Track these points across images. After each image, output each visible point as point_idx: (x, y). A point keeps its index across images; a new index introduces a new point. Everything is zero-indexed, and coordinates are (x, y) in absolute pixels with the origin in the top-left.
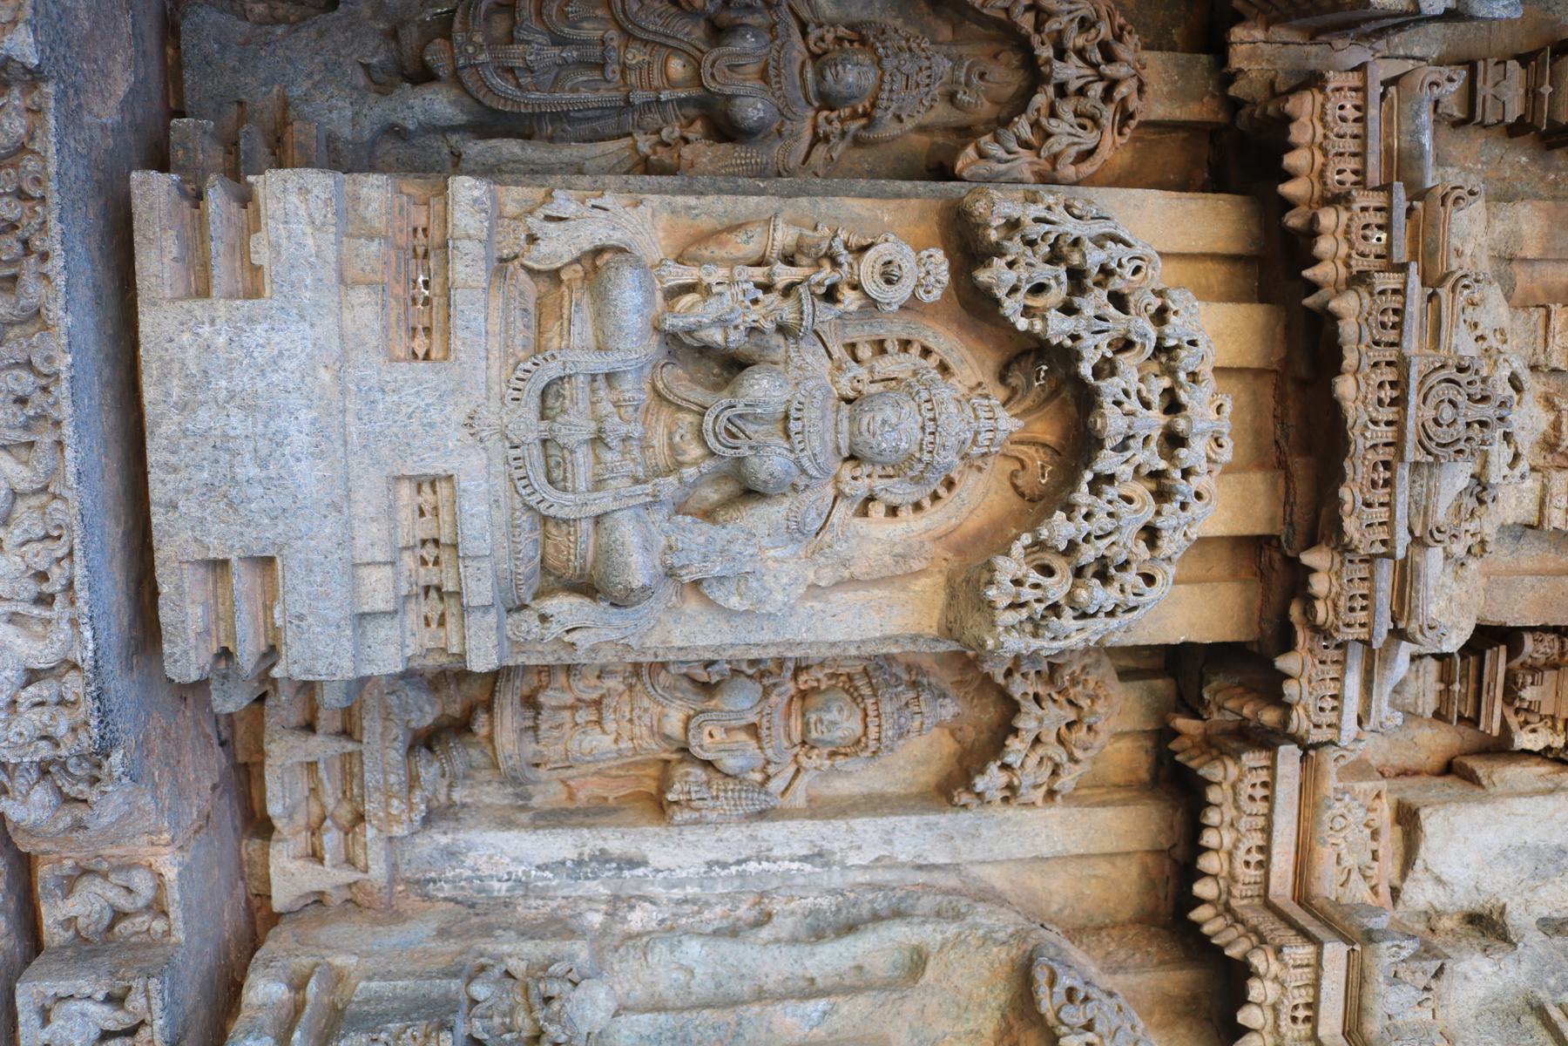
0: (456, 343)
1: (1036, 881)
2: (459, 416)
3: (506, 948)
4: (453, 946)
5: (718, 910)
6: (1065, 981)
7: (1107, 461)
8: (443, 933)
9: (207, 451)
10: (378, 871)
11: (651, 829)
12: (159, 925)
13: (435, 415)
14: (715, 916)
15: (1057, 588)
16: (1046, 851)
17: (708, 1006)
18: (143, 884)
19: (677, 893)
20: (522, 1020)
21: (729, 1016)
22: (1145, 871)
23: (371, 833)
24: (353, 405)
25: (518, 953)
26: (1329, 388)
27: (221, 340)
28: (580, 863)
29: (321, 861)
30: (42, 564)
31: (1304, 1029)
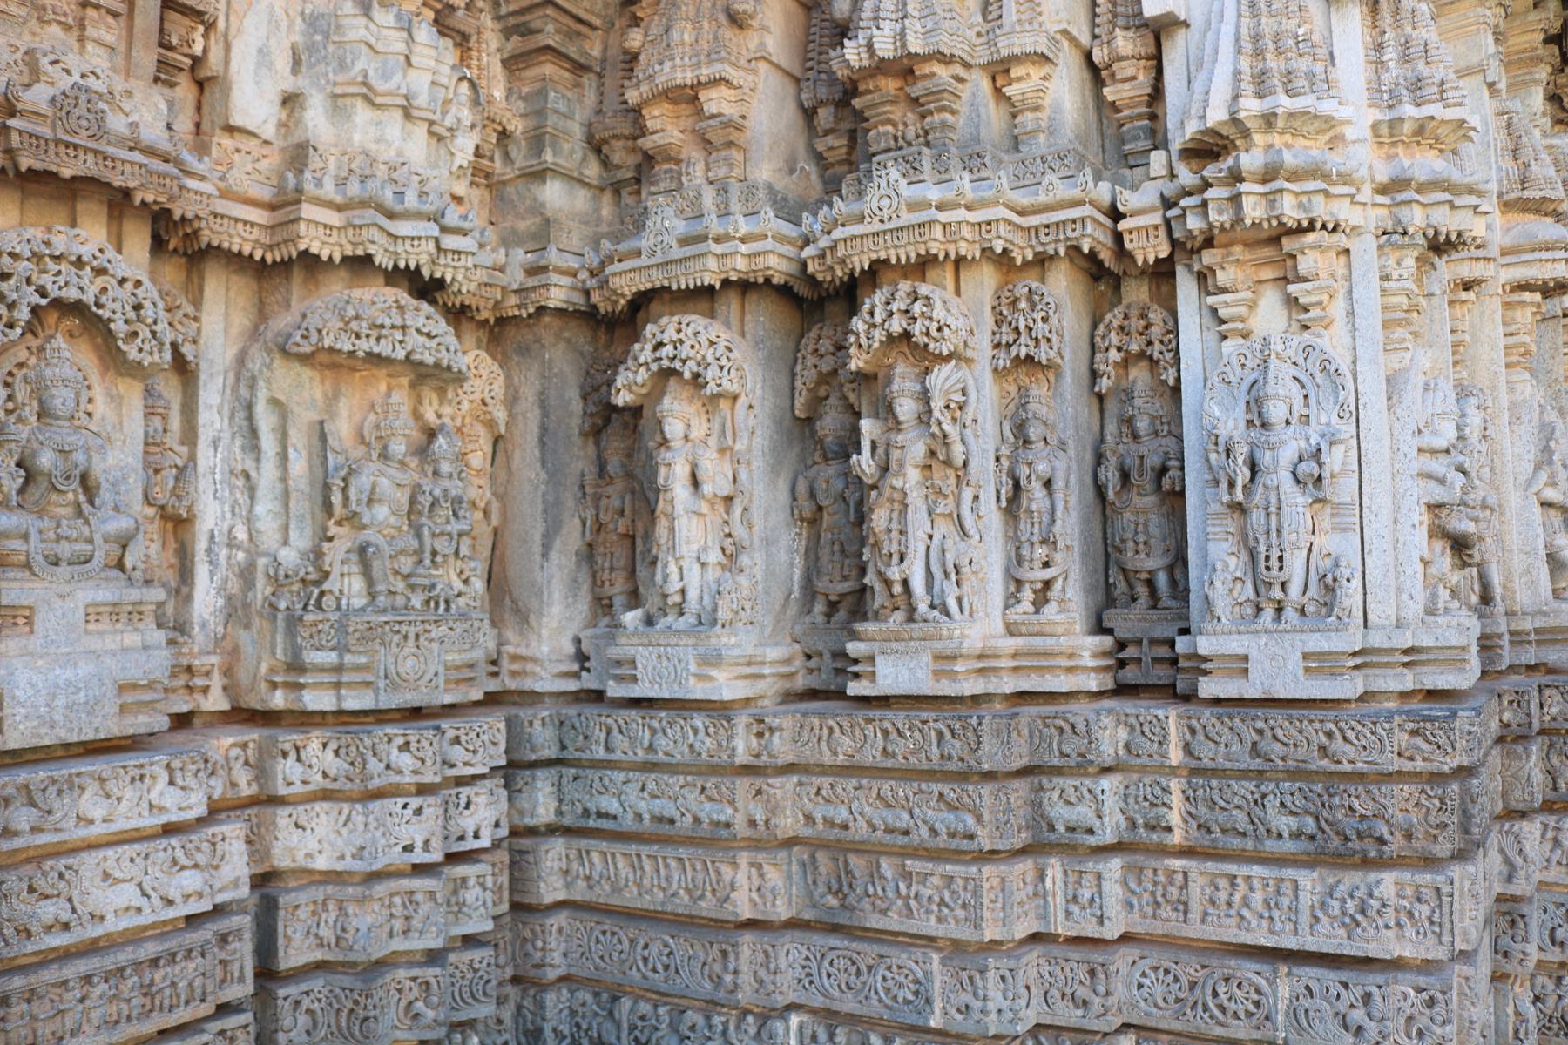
0: (26, 603)
1: (234, 331)
2: (59, 602)
3: (259, 596)
4: (256, 621)
5: (238, 495)
6: (298, 339)
7: (89, 298)
8: (247, 626)
9: (73, 715)
10: (214, 659)
11: (197, 527)
12: (251, 745)
13: (59, 613)
14: (242, 499)
15: (144, 332)
16: (222, 326)
17: (287, 505)
18: (235, 752)
19: (228, 515)
20: (295, 588)
21: (293, 495)
22: (235, 272)
23: (197, 662)
24: (52, 650)
25: (262, 589)
26: (65, 180)
27: (23, 711)
28: (211, 562)
29: (208, 687)
30: (128, 779)
31: (335, 232)
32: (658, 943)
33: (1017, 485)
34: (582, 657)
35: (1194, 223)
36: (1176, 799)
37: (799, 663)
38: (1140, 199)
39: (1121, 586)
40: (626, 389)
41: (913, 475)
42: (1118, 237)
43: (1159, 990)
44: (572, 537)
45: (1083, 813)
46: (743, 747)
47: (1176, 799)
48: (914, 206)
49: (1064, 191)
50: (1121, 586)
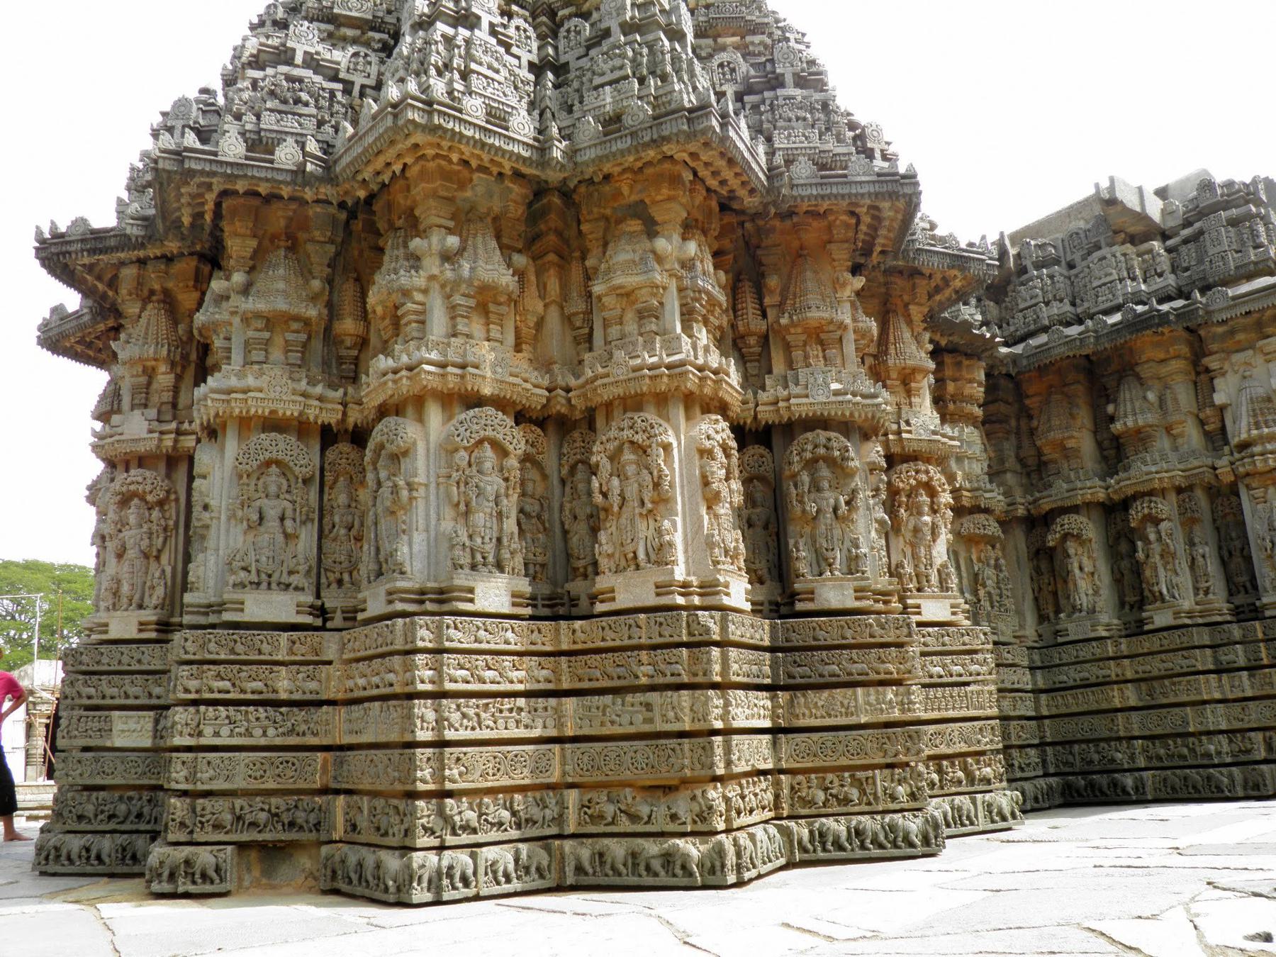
32: (1086, 721)
33: (1193, 559)
34: (1040, 636)
35: (1241, 470)
36: (1263, 649)
37: (1122, 627)
38: (1223, 463)
39: (1234, 589)
40: (1051, 540)
41: (1158, 557)
42: (1216, 476)
43: (1268, 714)
44: (1029, 596)
45: (1231, 657)
46: (1111, 650)
47: (1263, 649)
48: (1147, 474)
49: (1196, 463)
50: (1234, 589)
